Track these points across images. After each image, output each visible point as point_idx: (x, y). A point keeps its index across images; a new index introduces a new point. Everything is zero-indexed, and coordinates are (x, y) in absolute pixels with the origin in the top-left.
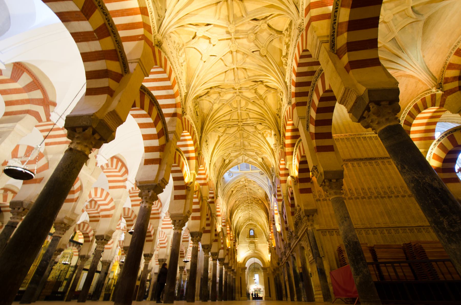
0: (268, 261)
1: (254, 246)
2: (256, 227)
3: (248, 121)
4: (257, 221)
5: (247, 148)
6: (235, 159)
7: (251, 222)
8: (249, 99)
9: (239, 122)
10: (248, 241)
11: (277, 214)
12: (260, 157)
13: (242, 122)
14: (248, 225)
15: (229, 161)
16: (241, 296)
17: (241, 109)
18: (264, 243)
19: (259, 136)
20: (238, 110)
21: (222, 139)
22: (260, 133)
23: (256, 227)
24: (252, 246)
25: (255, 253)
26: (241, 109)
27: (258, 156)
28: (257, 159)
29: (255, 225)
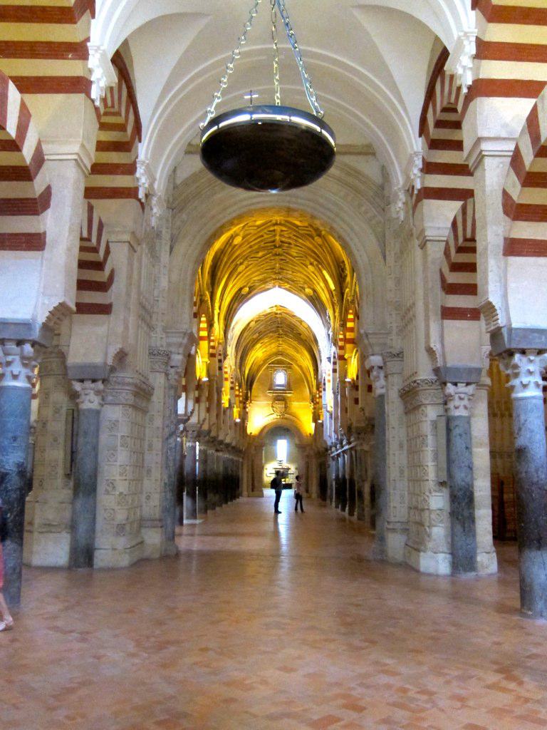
0: (310, 434)
1: (283, 406)
2: (290, 368)
3: (291, 248)
4: (292, 359)
5: (287, 273)
6: (260, 285)
7: (280, 357)
8: (297, 226)
9: (275, 247)
10: (271, 395)
11: (329, 381)
12: (309, 287)
13: (280, 247)
14: (273, 363)
15: (250, 288)
16: (253, 490)
17: (282, 233)
18: (304, 399)
19: (310, 267)
20: (275, 235)
21: (241, 268)
22: (311, 264)
23: (290, 368)
24: (280, 406)
25: (286, 419)
26: (282, 233)
27: (306, 286)
28: (304, 288)
29: (289, 363)
